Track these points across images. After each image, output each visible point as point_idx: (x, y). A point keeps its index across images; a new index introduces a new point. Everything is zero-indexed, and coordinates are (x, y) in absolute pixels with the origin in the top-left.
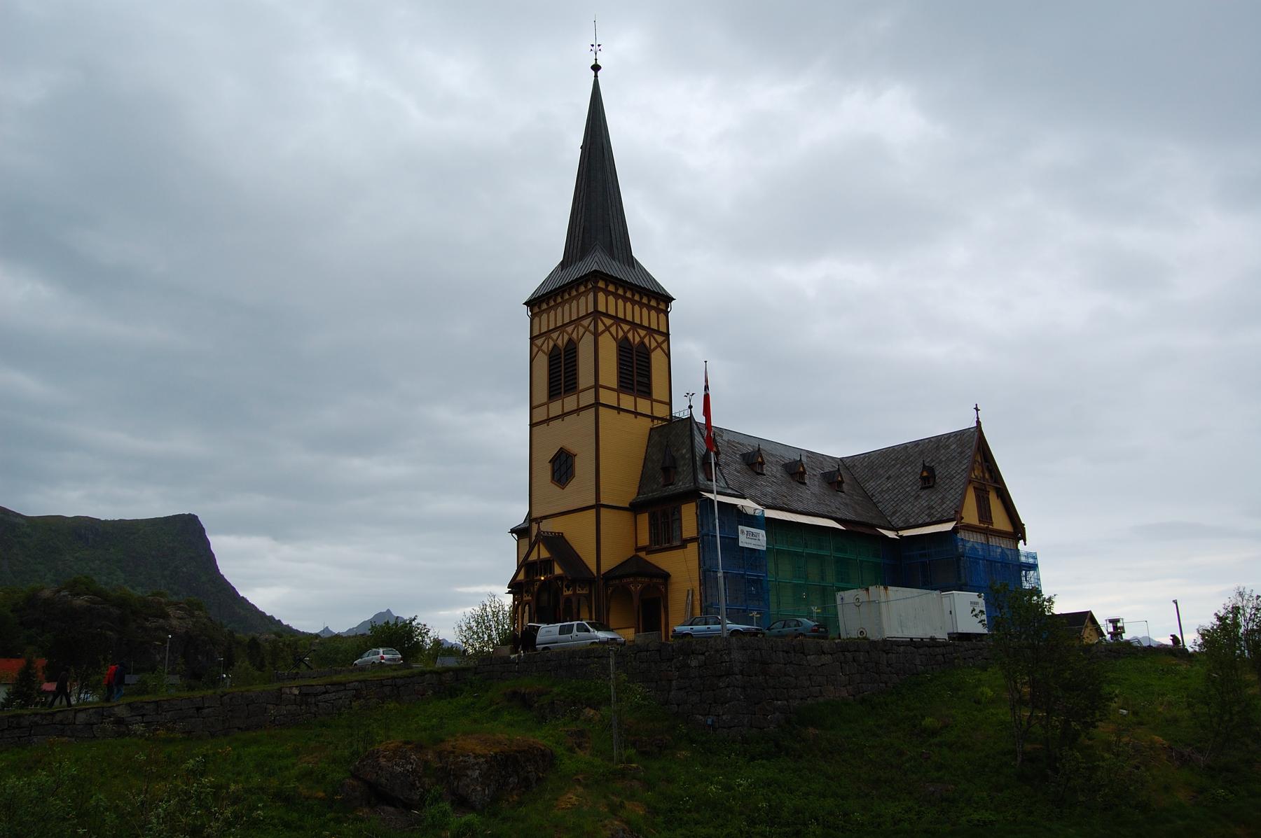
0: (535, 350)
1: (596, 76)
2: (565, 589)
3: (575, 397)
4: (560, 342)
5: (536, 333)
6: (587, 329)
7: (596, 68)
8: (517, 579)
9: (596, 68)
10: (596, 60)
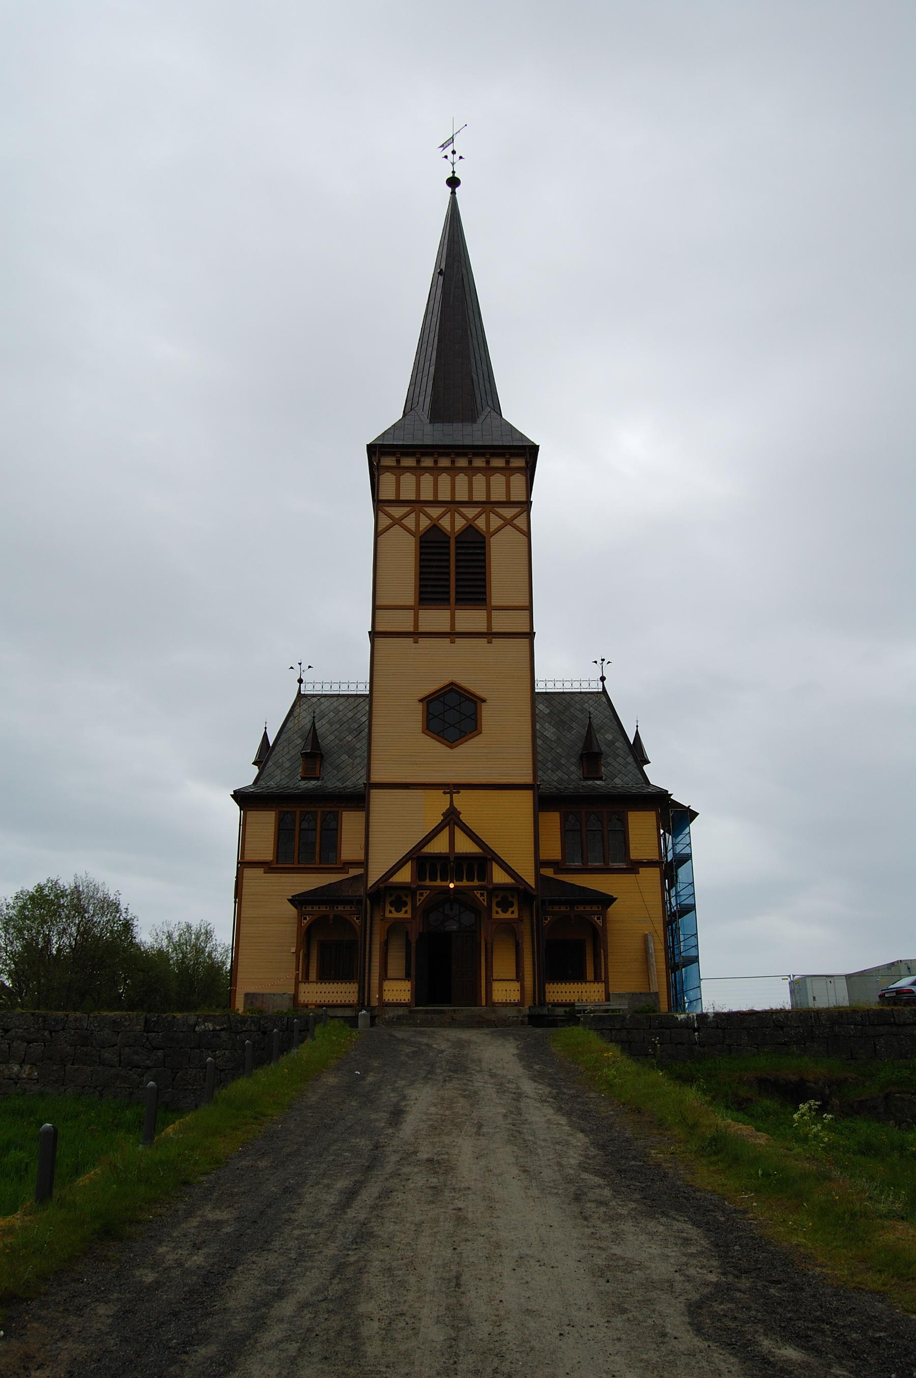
0: (385, 521)
1: (453, 193)
2: (495, 908)
3: (483, 613)
4: (445, 523)
6: (509, 522)
7: (453, 182)
8: (391, 880)
9: (453, 182)
10: (454, 172)
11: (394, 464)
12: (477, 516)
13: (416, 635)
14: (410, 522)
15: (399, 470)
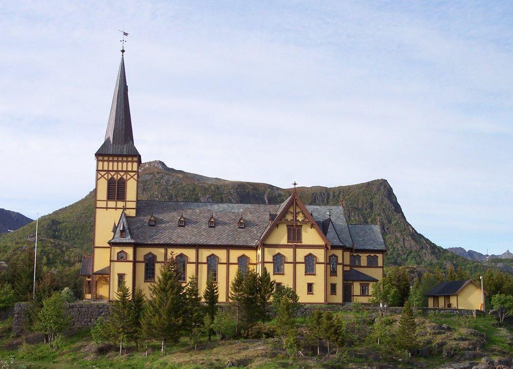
0: (99, 176)
4: (115, 177)
5: (100, 168)
6: (132, 177)
7: (123, 51)
9: (123, 51)
11: (102, 159)
12: (124, 174)
13: (107, 208)
14: (106, 176)
15: (103, 161)
